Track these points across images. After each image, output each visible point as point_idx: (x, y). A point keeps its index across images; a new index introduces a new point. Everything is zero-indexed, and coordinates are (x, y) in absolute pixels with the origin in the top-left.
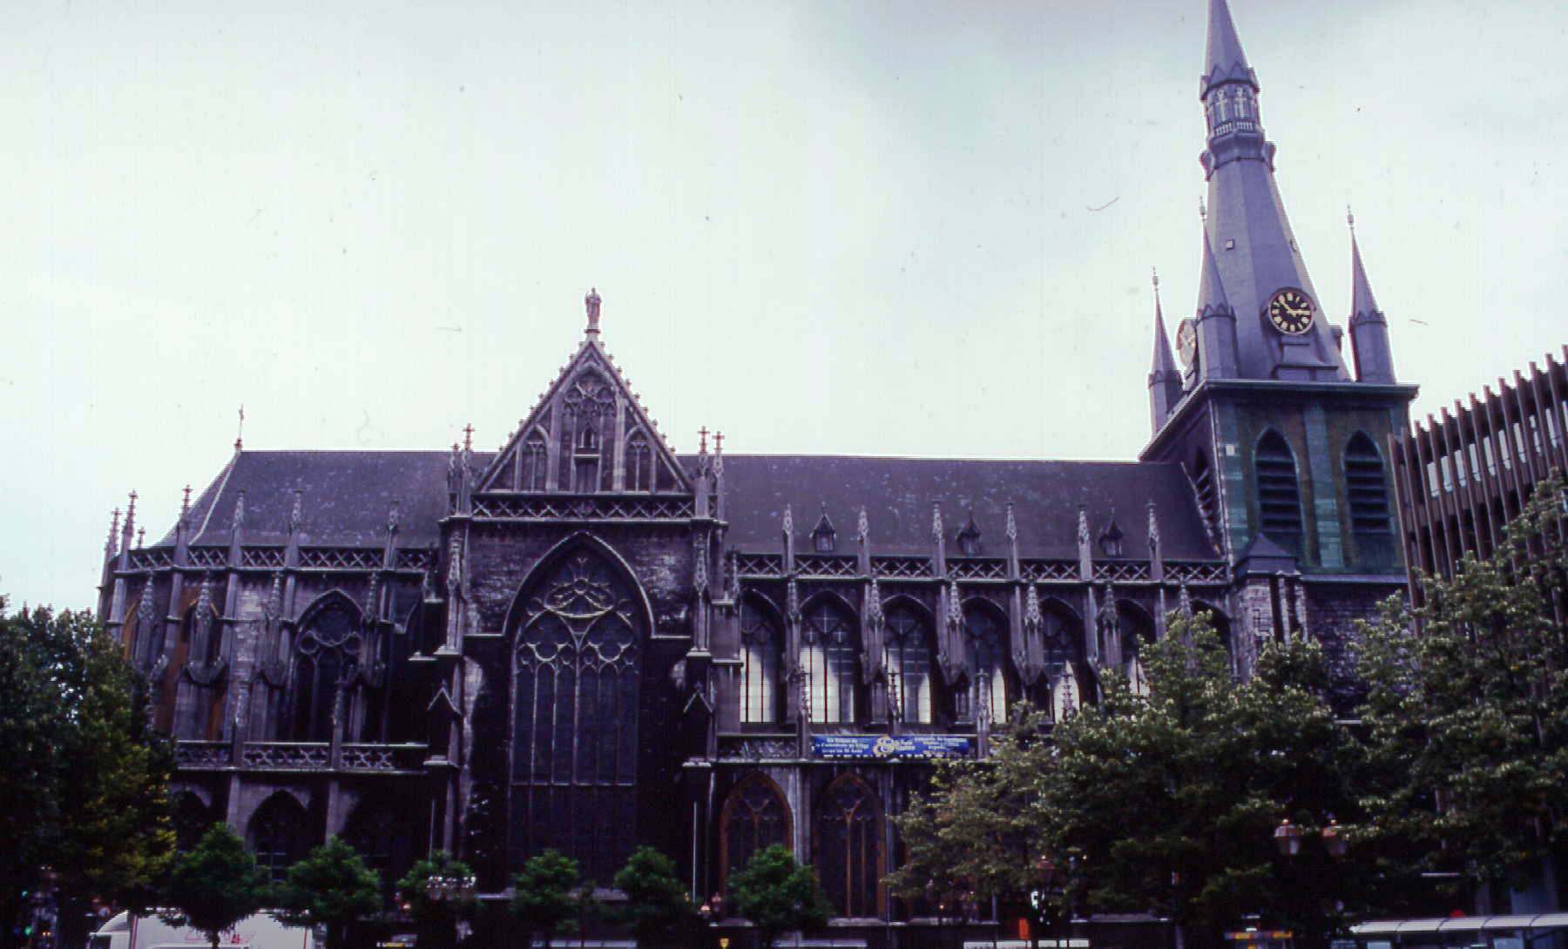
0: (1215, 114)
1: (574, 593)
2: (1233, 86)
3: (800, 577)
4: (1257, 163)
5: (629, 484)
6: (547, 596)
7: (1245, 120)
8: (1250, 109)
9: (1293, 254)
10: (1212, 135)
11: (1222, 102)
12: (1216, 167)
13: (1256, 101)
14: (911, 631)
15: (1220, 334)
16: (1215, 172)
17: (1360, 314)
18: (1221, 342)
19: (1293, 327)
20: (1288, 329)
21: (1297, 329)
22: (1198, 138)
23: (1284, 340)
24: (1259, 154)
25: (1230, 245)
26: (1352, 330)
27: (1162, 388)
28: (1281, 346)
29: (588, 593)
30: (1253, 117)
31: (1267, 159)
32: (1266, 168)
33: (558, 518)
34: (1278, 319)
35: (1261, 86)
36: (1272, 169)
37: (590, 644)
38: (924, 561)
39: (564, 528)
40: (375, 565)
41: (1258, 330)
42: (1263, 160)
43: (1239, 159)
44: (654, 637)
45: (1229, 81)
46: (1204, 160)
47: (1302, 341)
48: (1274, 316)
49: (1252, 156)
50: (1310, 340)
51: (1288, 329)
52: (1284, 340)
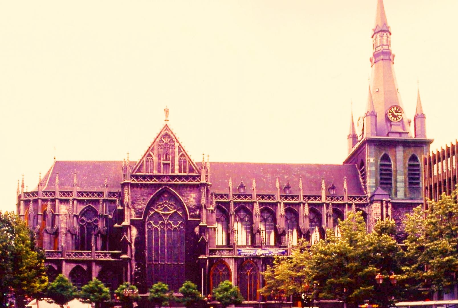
0: (376, 43)
1: (164, 206)
2: (383, 32)
3: (235, 201)
4: (388, 61)
5: (180, 171)
6: (155, 206)
7: (386, 45)
8: (388, 41)
9: (398, 94)
10: (374, 51)
11: (379, 38)
12: (375, 63)
13: (390, 38)
15: (371, 121)
16: (374, 64)
17: (418, 114)
18: (371, 124)
19: (395, 119)
20: (394, 120)
21: (397, 120)
22: (370, 52)
23: (392, 123)
24: (390, 58)
25: (377, 90)
26: (415, 120)
28: (391, 125)
29: (168, 206)
31: (392, 60)
32: (391, 63)
33: (158, 182)
34: (391, 116)
36: (393, 63)
37: (169, 221)
38: (273, 196)
39: (160, 185)
40: (101, 197)
41: (384, 120)
42: (391, 60)
43: (382, 60)
44: (189, 219)
45: (381, 31)
46: (371, 60)
47: (398, 124)
48: (389, 115)
49: (387, 59)
50: (401, 123)
51: (394, 120)
52: (392, 123)
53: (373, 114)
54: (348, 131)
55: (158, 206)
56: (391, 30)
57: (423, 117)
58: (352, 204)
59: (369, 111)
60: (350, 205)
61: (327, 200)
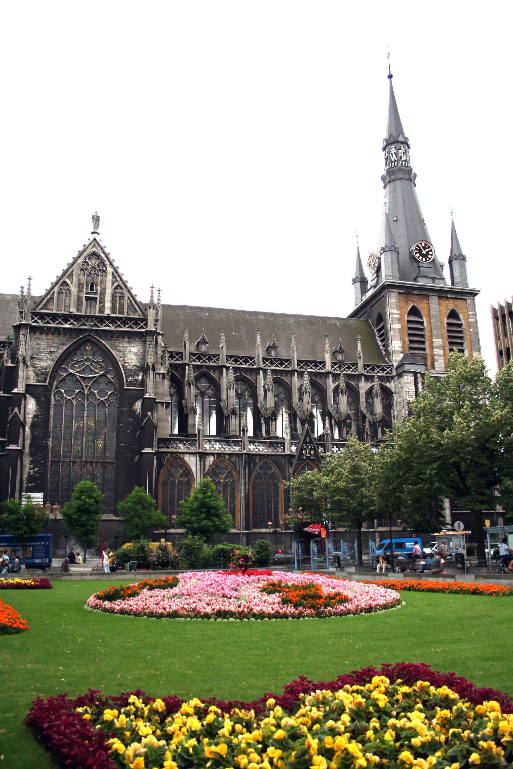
4: (408, 181)
6: (70, 365)
7: (404, 161)
10: (388, 167)
11: (393, 152)
12: (389, 182)
15: (392, 259)
17: (455, 255)
18: (392, 263)
19: (424, 259)
20: (422, 260)
21: (426, 260)
22: (381, 169)
23: (420, 265)
25: (395, 219)
26: (450, 263)
27: (358, 285)
28: (419, 267)
30: (406, 160)
32: (413, 185)
34: (418, 255)
35: (411, 146)
36: (415, 186)
38: (251, 358)
41: (408, 260)
46: (383, 178)
47: (428, 266)
48: (416, 253)
51: (422, 260)
52: (420, 265)
53: (393, 249)
54: (353, 273)
55: (75, 364)
56: (411, 142)
57: (462, 258)
59: (388, 245)
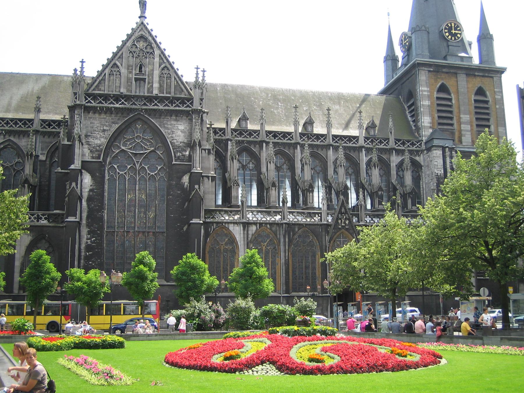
6: (122, 142)
14: (249, 163)
19: (453, 38)
20: (451, 39)
21: (455, 39)
23: (449, 43)
27: (390, 63)
28: (448, 46)
34: (447, 34)
47: (457, 45)
48: (446, 33)
50: (460, 44)
51: (451, 39)
52: (449, 43)
53: (423, 28)
54: (383, 53)
55: (126, 141)
57: (491, 38)
58: (338, 147)
60: (267, 143)
61: (334, 141)
